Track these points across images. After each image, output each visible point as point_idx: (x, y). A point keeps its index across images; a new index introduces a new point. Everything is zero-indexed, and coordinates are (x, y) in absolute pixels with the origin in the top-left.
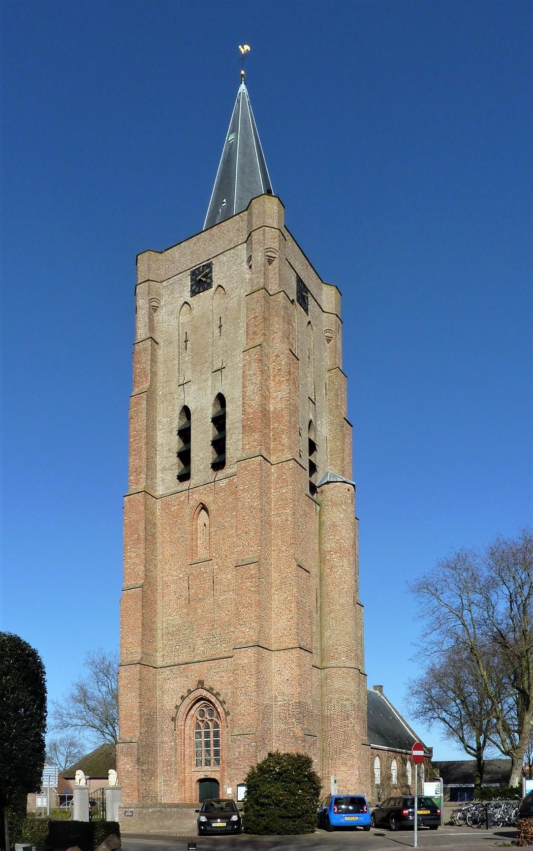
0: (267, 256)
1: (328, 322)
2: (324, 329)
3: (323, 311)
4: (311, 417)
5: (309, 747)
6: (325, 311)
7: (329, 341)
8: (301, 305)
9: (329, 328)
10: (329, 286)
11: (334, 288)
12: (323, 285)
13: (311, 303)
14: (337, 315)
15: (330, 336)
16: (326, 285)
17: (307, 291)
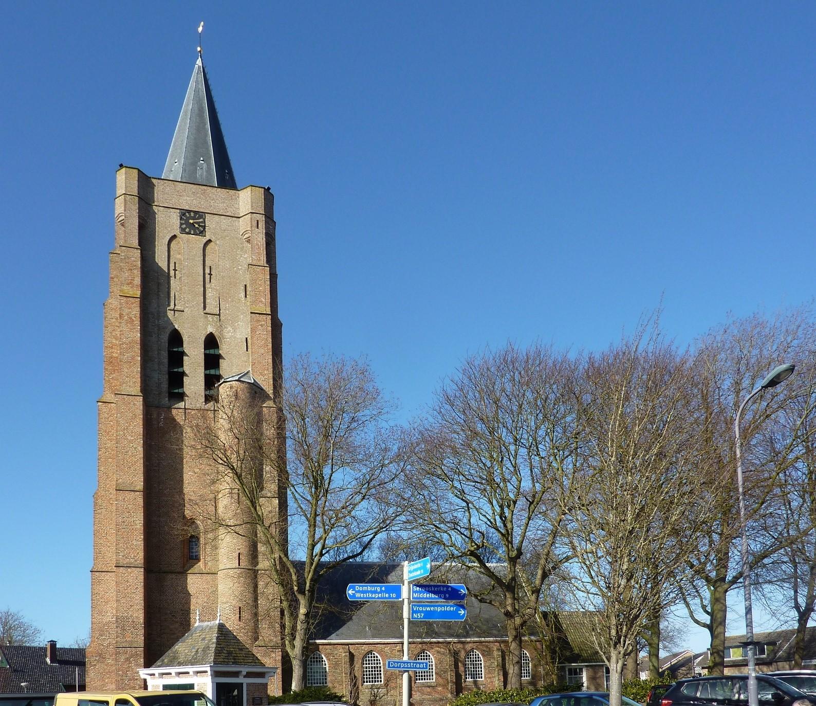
0: (119, 222)
1: (244, 224)
2: (241, 234)
3: (239, 218)
4: (210, 329)
5: (127, 659)
6: (239, 216)
7: (249, 241)
8: (189, 233)
9: (245, 230)
10: (245, 190)
11: (249, 189)
12: (240, 192)
13: (210, 222)
14: (251, 213)
15: (248, 236)
16: (242, 191)
17: (200, 215)
